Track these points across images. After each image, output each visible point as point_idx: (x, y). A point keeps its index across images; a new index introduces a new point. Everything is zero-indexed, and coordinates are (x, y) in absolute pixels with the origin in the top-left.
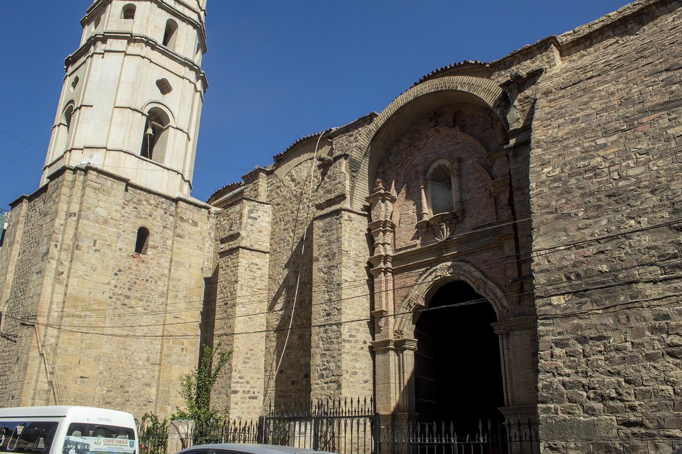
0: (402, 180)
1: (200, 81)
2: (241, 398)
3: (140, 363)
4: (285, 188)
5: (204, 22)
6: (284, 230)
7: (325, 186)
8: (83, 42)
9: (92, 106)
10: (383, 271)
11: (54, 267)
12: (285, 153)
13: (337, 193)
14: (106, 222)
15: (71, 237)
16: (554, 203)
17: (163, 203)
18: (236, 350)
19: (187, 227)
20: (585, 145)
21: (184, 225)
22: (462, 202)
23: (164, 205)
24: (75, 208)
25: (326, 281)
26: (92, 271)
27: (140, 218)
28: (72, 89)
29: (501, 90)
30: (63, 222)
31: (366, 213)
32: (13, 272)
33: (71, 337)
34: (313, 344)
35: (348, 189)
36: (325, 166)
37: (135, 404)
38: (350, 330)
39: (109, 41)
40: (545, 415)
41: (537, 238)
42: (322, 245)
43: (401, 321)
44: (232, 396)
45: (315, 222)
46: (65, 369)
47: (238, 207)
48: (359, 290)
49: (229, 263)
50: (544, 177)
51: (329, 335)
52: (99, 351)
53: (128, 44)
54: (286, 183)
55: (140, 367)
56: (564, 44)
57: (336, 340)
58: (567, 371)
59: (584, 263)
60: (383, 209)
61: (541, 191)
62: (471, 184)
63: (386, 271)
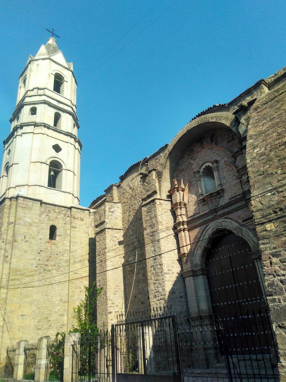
0: (187, 178)
1: (77, 143)
5: (75, 111)
7: (146, 188)
8: (12, 130)
9: (18, 164)
10: (182, 230)
11: (3, 254)
12: (124, 174)
13: (152, 191)
15: (11, 236)
16: (262, 169)
18: (109, 288)
19: (78, 222)
20: (279, 131)
21: (76, 221)
22: (221, 185)
23: (63, 212)
24: (12, 219)
25: (152, 240)
26: (24, 253)
27: (51, 220)
28: (8, 156)
29: (234, 116)
30: (6, 228)
31: (170, 200)
33: (15, 292)
34: (149, 278)
35: (158, 187)
36: (144, 177)
38: (168, 267)
39: (24, 128)
40: (272, 304)
41: (253, 191)
42: (147, 220)
44: (109, 315)
45: (143, 208)
46: (12, 312)
47: (103, 207)
48: (170, 243)
49: (101, 238)
50: (255, 155)
51: (156, 271)
52: (32, 298)
53: (35, 127)
54: (127, 191)
55: (56, 305)
56: (270, 83)
57: (160, 274)
58: (282, 272)
59: (284, 201)
60: (178, 195)
61: (253, 163)
62: (225, 173)
63: (184, 230)
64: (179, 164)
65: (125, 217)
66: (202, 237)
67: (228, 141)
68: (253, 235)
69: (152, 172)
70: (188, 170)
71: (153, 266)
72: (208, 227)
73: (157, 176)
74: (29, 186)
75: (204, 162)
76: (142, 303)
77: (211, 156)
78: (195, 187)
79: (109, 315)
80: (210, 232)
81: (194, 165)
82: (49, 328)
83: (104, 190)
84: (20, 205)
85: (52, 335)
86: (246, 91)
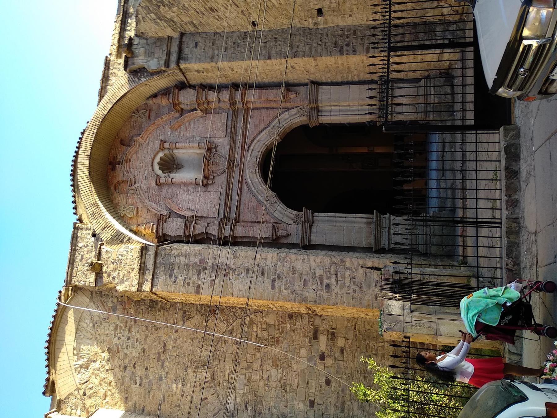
6: (140, 385)
7: (121, 277)
42: (185, 280)
43: (287, 216)
62: (188, 134)
64: (122, 215)
66: (259, 197)
67: (147, 119)
68: (287, 113)
69: (103, 251)
70: (144, 198)
71: (274, 280)
72: (249, 180)
73: (116, 245)
75: (150, 164)
76: (328, 382)
77: (149, 150)
78: (178, 192)
80: (257, 180)
81: (142, 185)
86: (102, 79)
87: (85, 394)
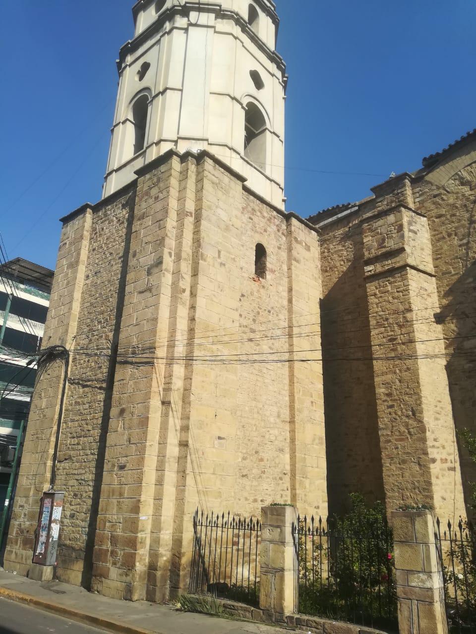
2: (440, 469)
3: (272, 420)
4: (449, 195)
6: (460, 246)
12: (444, 151)
14: (227, 229)
17: (275, 218)
23: (276, 220)
27: (256, 232)
28: (137, 78)
30: (175, 224)
32: (80, 300)
37: (271, 477)
39: (193, 15)
44: (432, 466)
47: (391, 218)
49: (389, 288)
53: (216, 18)
55: (272, 426)
65: (445, 247)
74: (209, 144)
79: (432, 466)
82: (261, 477)
83: (372, 187)
84: (209, 174)
85: (267, 494)
87: (435, 196)
